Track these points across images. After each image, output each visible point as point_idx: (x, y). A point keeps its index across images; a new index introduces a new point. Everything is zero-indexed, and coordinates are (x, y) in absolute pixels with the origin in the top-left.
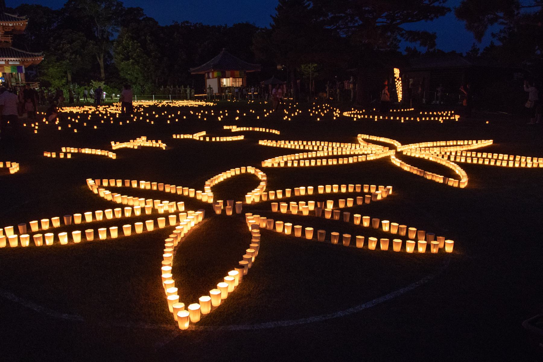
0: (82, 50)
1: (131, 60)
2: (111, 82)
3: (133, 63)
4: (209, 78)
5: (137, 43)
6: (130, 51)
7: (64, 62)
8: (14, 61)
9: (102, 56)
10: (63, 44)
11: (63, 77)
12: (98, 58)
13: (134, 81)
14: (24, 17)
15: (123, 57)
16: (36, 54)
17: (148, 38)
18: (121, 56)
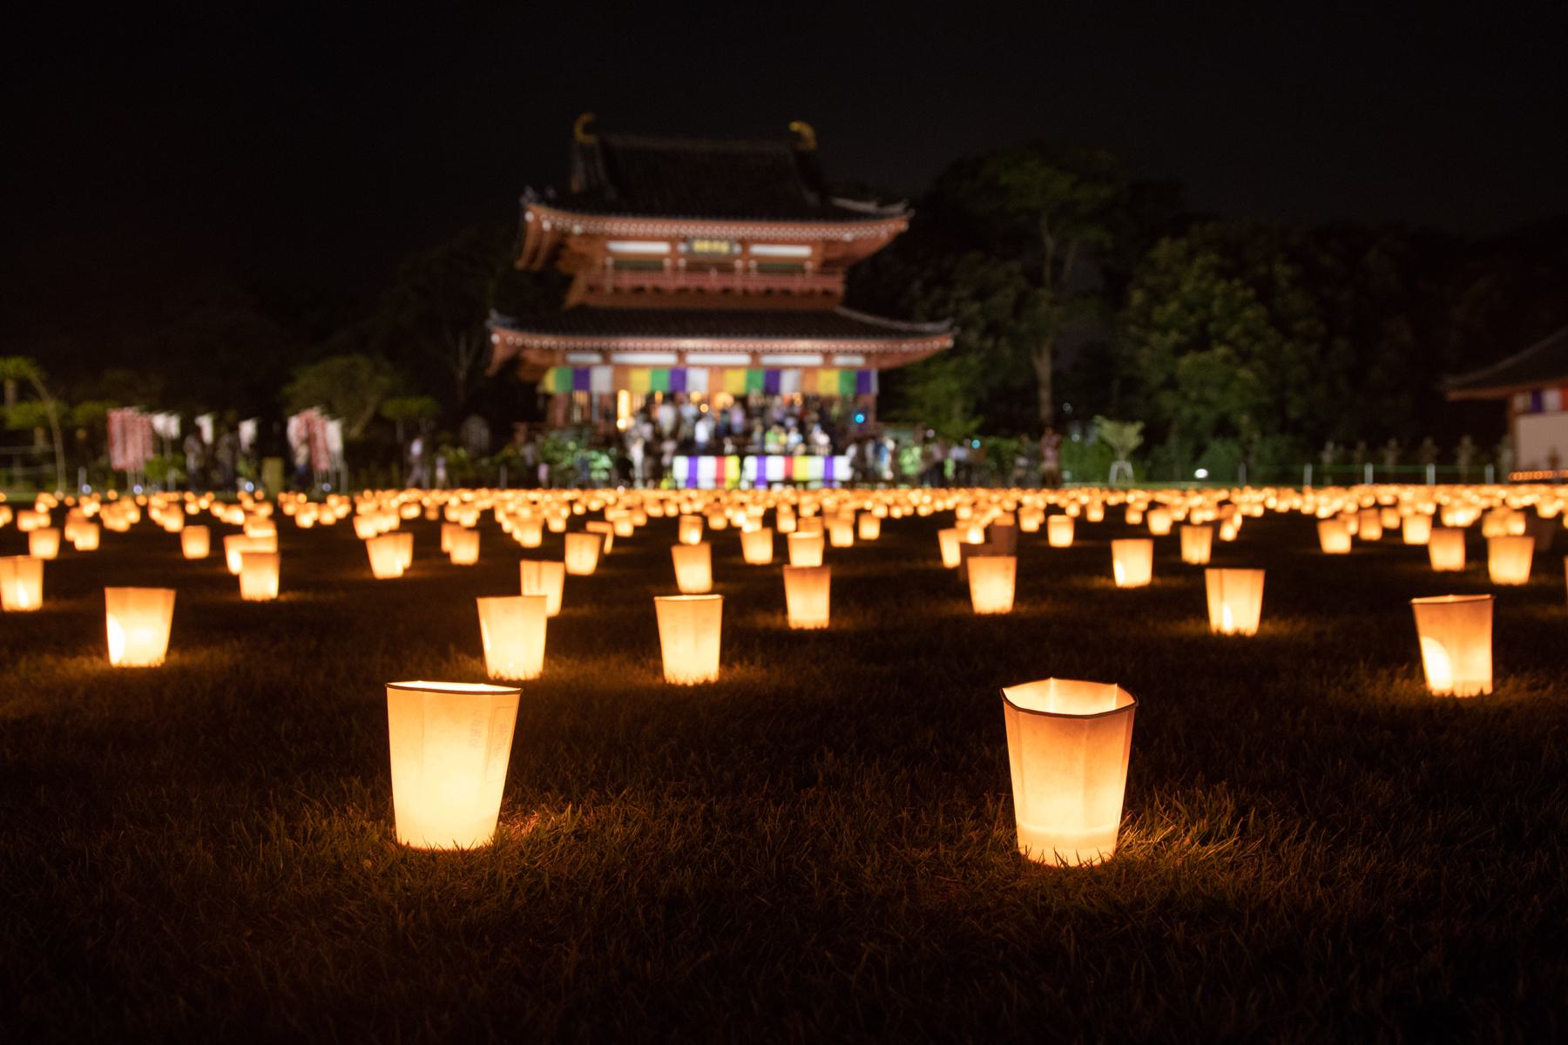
4: (1537, 408)
8: (851, 355)
10: (959, 301)
14: (898, 208)
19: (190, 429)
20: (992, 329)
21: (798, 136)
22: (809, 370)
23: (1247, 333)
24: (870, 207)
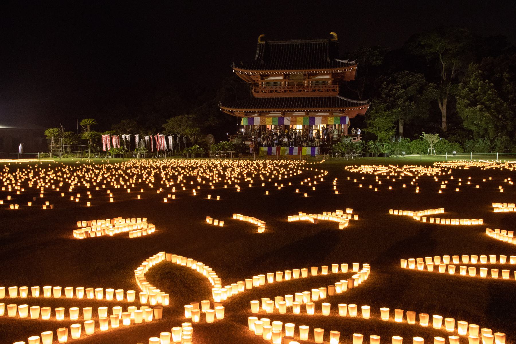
0: (419, 96)
1: (479, 106)
2: (454, 134)
3: (481, 110)
5: (489, 83)
6: (479, 94)
7: (395, 111)
9: (445, 101)
10: (396, 89)
11: (391, 128)
12: (440, 105)
13: (481, 133)
14: (353, 62)
15: (469, 102)
16: (361, 102)
17: (506, 75)
18: (466, 101)
19: (133, 138)
20: (410, 99)
21: (332, 35)
22: (323, 117)
23: (489, 99)
24: (346, 62)
